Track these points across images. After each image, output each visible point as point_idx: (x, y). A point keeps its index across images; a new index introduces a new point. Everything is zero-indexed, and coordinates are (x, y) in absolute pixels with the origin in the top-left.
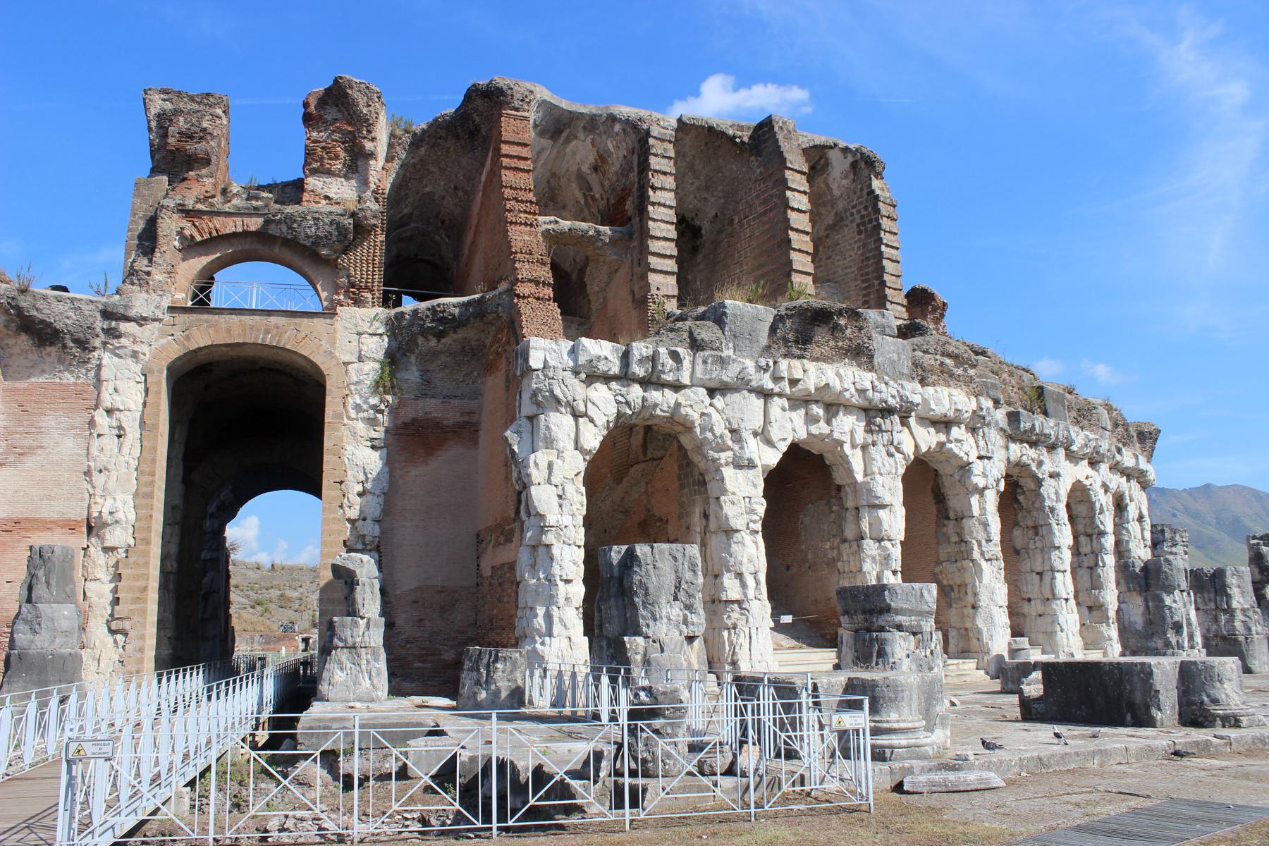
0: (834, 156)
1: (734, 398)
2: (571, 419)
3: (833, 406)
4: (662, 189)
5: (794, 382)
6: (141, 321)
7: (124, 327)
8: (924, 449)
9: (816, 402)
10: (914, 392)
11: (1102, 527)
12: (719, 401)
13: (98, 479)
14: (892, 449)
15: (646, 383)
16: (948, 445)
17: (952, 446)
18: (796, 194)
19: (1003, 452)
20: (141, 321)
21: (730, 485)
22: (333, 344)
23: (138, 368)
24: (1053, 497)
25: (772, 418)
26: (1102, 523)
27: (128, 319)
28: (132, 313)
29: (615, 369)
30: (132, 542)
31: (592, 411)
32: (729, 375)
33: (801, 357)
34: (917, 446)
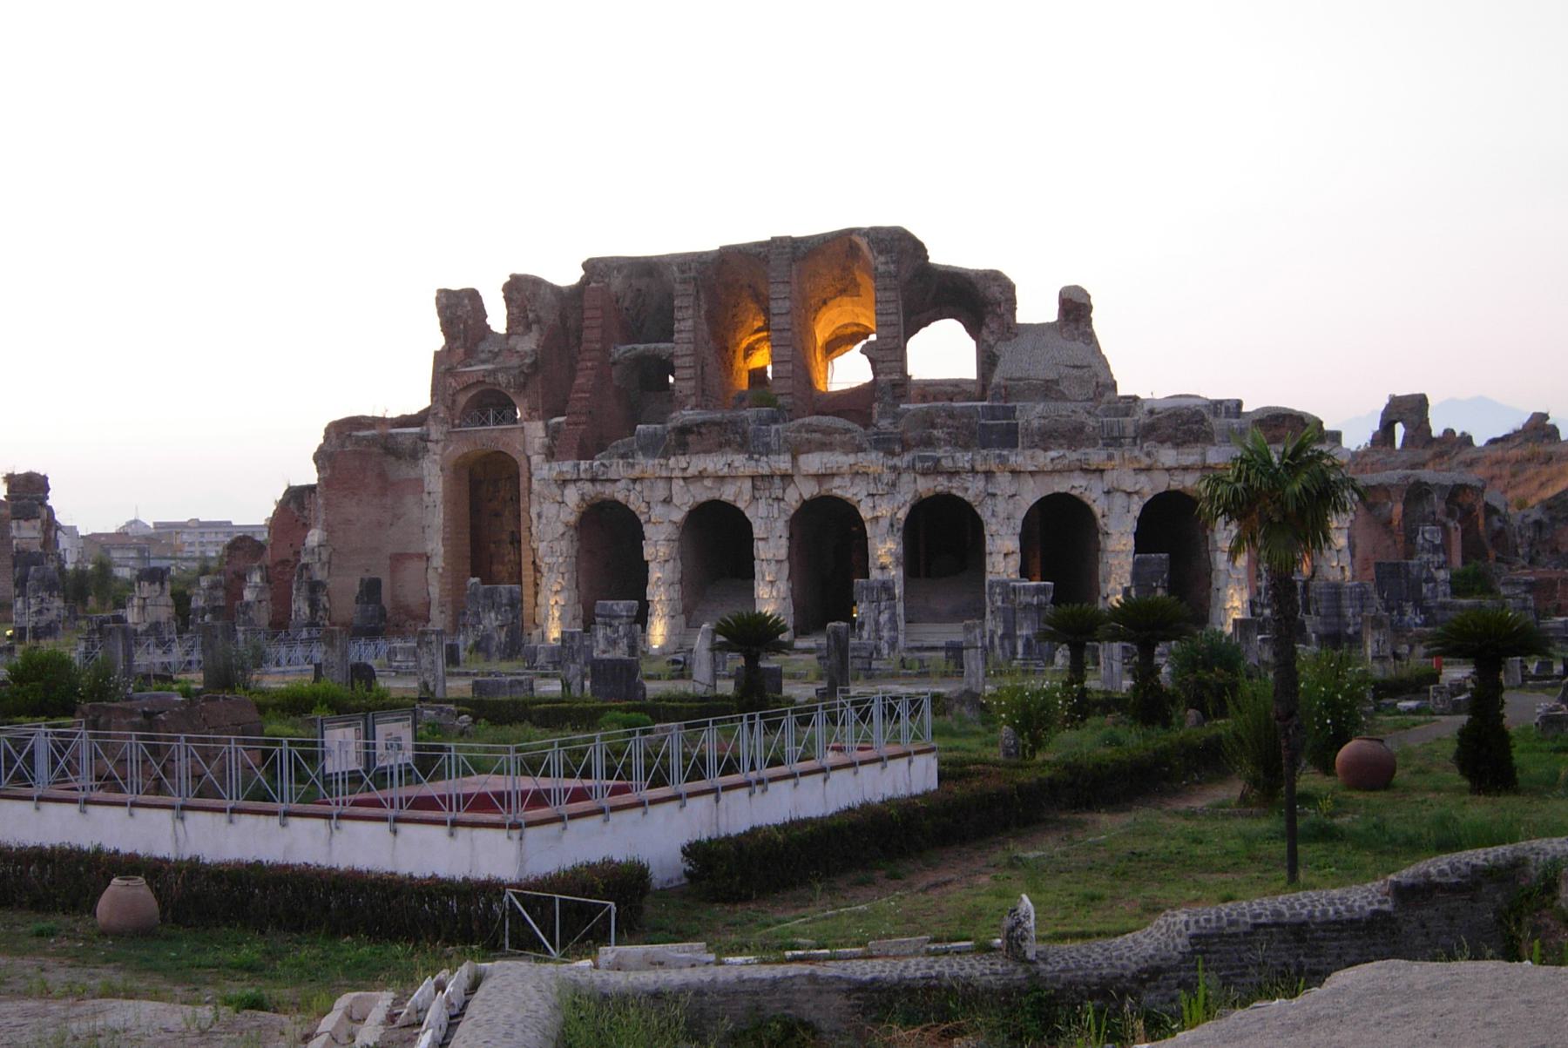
0: (855, 238)
1: (647, 483)
2: (557, 505)
3: (720, 479)
4: (684, 319)
5: (685, 469)
6: (437, 442)
7: (429, 444)
8: (806, 496)
9: (708, 477)
10: (783, 463)
11: (1106, 529)
12: (638, 487)
13: (427, 530)
14: (770, 501)
15: (593, 480)
16: (834, 491)
17: (838, 492)
18: (780, 302)
19: (912, 486)
20: (437, 442)
21: (647, 535)
22: (524, 443)
23: (438, 468)
24: (989, 513)
25: (673, 492)
26: (1106, 525)
27: (431, 441)
28: (431, 438)
29: (575, 477)
30: (443, 565)
31: (567, 500)
32: (636, 473)
33: (684, 454)
34: (801, 494)
